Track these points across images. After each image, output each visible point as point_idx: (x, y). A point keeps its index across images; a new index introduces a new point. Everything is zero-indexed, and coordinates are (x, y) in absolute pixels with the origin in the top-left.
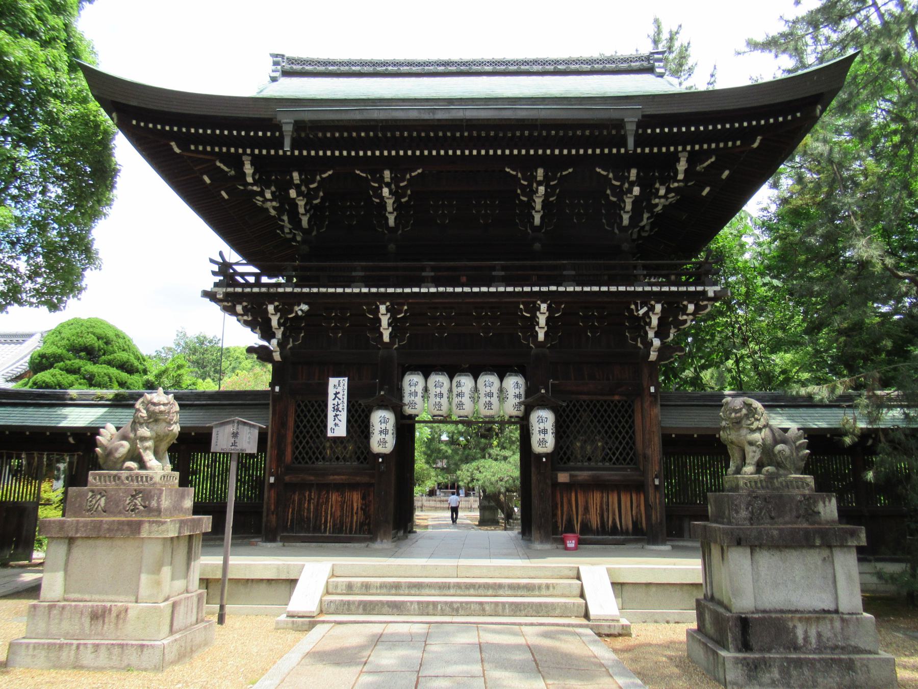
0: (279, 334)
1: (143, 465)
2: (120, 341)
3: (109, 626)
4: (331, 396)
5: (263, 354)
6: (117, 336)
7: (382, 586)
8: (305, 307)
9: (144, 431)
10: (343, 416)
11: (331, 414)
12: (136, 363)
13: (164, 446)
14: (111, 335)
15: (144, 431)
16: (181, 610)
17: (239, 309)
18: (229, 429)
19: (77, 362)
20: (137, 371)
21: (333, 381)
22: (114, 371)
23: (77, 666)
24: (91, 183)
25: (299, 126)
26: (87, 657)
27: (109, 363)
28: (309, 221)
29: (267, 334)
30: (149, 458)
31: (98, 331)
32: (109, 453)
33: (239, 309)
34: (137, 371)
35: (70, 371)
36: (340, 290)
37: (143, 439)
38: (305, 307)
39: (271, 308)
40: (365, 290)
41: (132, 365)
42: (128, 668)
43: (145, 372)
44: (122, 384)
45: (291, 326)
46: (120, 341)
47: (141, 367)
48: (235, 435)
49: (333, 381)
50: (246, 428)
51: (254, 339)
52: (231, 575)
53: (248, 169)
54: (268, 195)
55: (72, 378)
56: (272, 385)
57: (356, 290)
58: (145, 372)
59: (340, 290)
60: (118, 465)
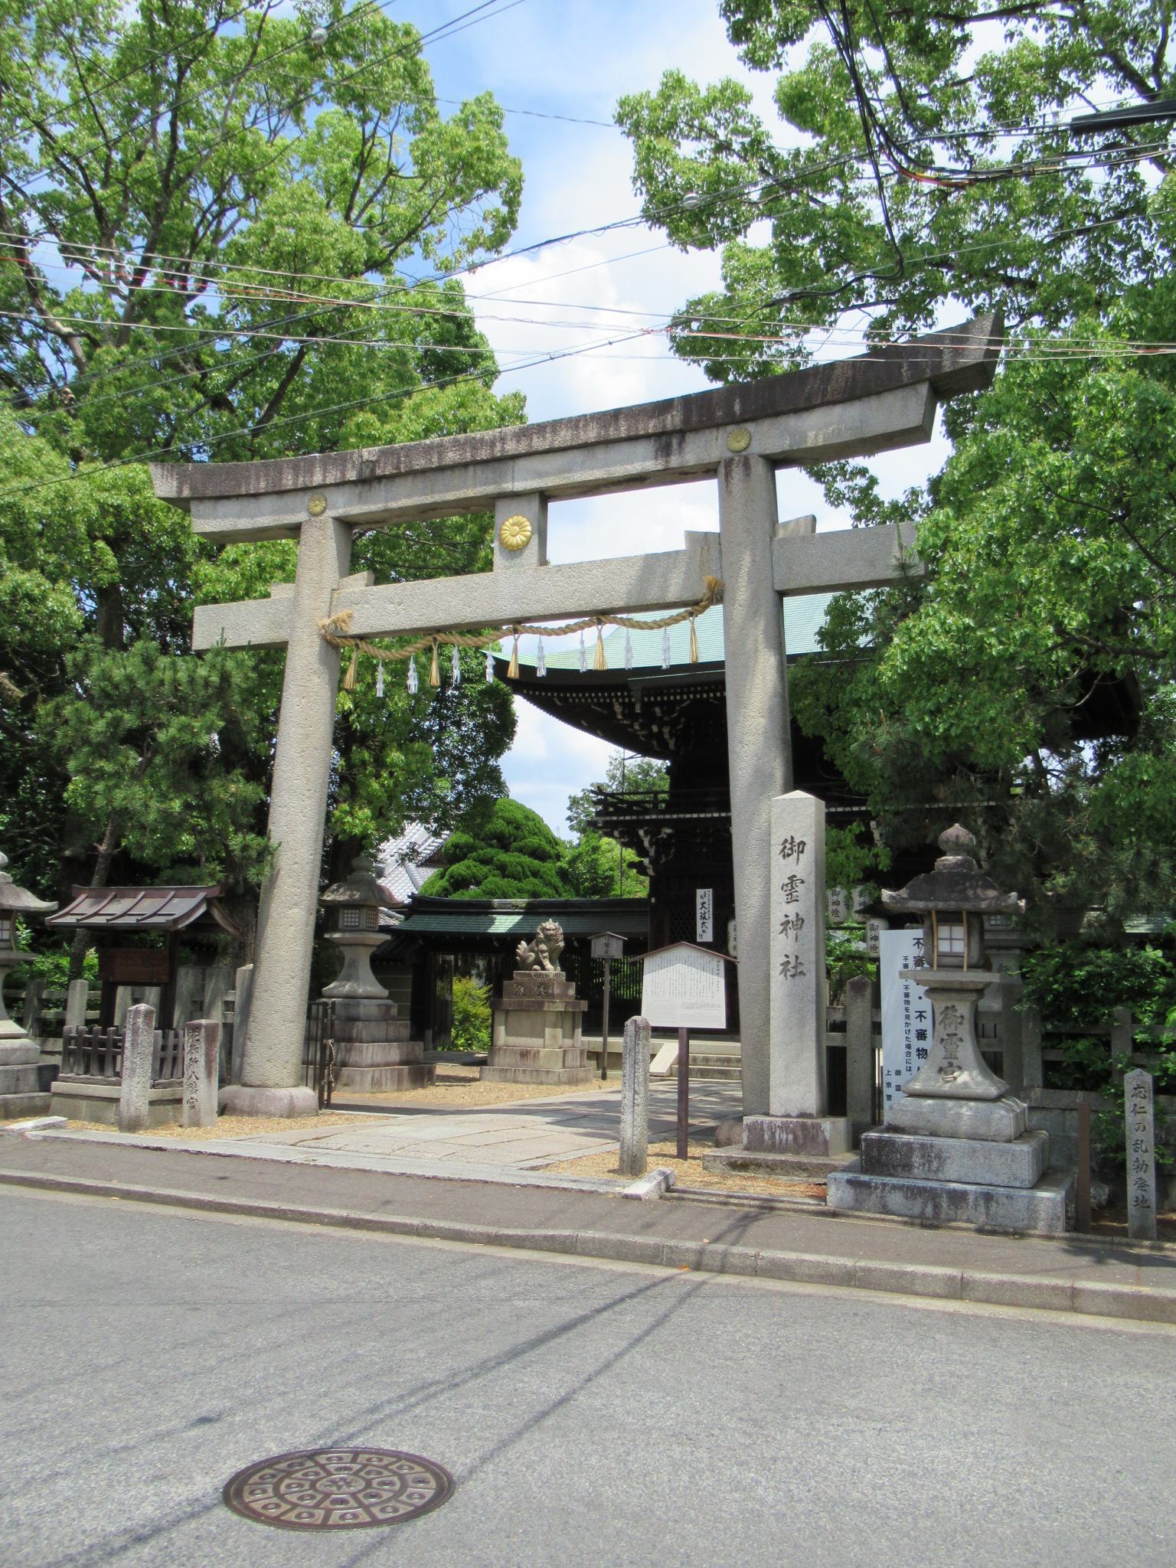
0: (652, 852)
1: (543, 968)
2: (530, 823)
3: (530, 1061)
4: (699, 906)
5: (641, 869)
6: (527, 818)
7: (718, 1060)
8: (669, 831)
9: (543, 947)
10: (710, 923)
11: (699, 922)
12: (548, 848)
13: (556, 955)
14: (519, 816)
15: (543, 947)
16: (569, 1056)
17: (616, 833)
18: (603, 940)
19: (490, 851)
20: (550, 857)
21: (700, 892)
22: (526, 860)
23: (516, 1082)
24: (501, 732)
25: (648, 690)
26: (520, 1077)
27: (521, 850)
28: (676, 744)
29: (642, 852)
30: (547, 963)
31: (507, 815)
32: (524, 960)
33: (616, 833)
34: (550, 857)
35: (485, 861)
36: (695, 816)
37: (543, 952)
38: (669, 831)
39: (641, 832)
40: (716, 815)
41: (544, 851)
42: (541, 1083)
43: (558, 857)
44: (535, 874)
45: (661, 845)
46: (530, 823)
47: (553, 852)
48: (607, 945)
49: (700, 892)
50: (613, 941)
51: (630, 854)
52: (609, 1050)
53: (618, 708)
54: (637, 727)
55: (485, 869)
56: (650, 895)
57: (709, 815)
58: (558, 857)
59: (695, 816)
60: (529, 967)
